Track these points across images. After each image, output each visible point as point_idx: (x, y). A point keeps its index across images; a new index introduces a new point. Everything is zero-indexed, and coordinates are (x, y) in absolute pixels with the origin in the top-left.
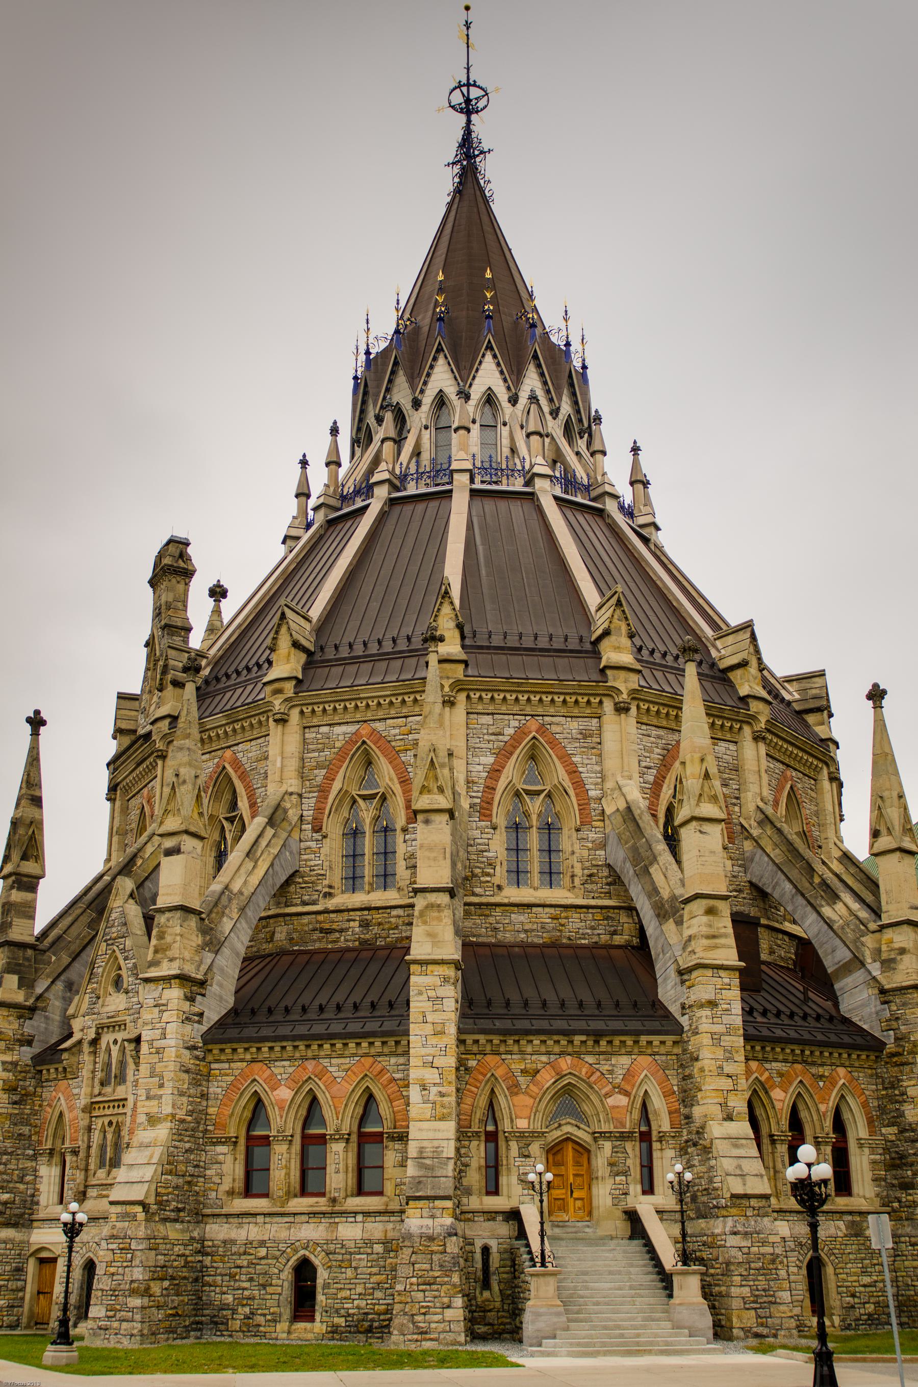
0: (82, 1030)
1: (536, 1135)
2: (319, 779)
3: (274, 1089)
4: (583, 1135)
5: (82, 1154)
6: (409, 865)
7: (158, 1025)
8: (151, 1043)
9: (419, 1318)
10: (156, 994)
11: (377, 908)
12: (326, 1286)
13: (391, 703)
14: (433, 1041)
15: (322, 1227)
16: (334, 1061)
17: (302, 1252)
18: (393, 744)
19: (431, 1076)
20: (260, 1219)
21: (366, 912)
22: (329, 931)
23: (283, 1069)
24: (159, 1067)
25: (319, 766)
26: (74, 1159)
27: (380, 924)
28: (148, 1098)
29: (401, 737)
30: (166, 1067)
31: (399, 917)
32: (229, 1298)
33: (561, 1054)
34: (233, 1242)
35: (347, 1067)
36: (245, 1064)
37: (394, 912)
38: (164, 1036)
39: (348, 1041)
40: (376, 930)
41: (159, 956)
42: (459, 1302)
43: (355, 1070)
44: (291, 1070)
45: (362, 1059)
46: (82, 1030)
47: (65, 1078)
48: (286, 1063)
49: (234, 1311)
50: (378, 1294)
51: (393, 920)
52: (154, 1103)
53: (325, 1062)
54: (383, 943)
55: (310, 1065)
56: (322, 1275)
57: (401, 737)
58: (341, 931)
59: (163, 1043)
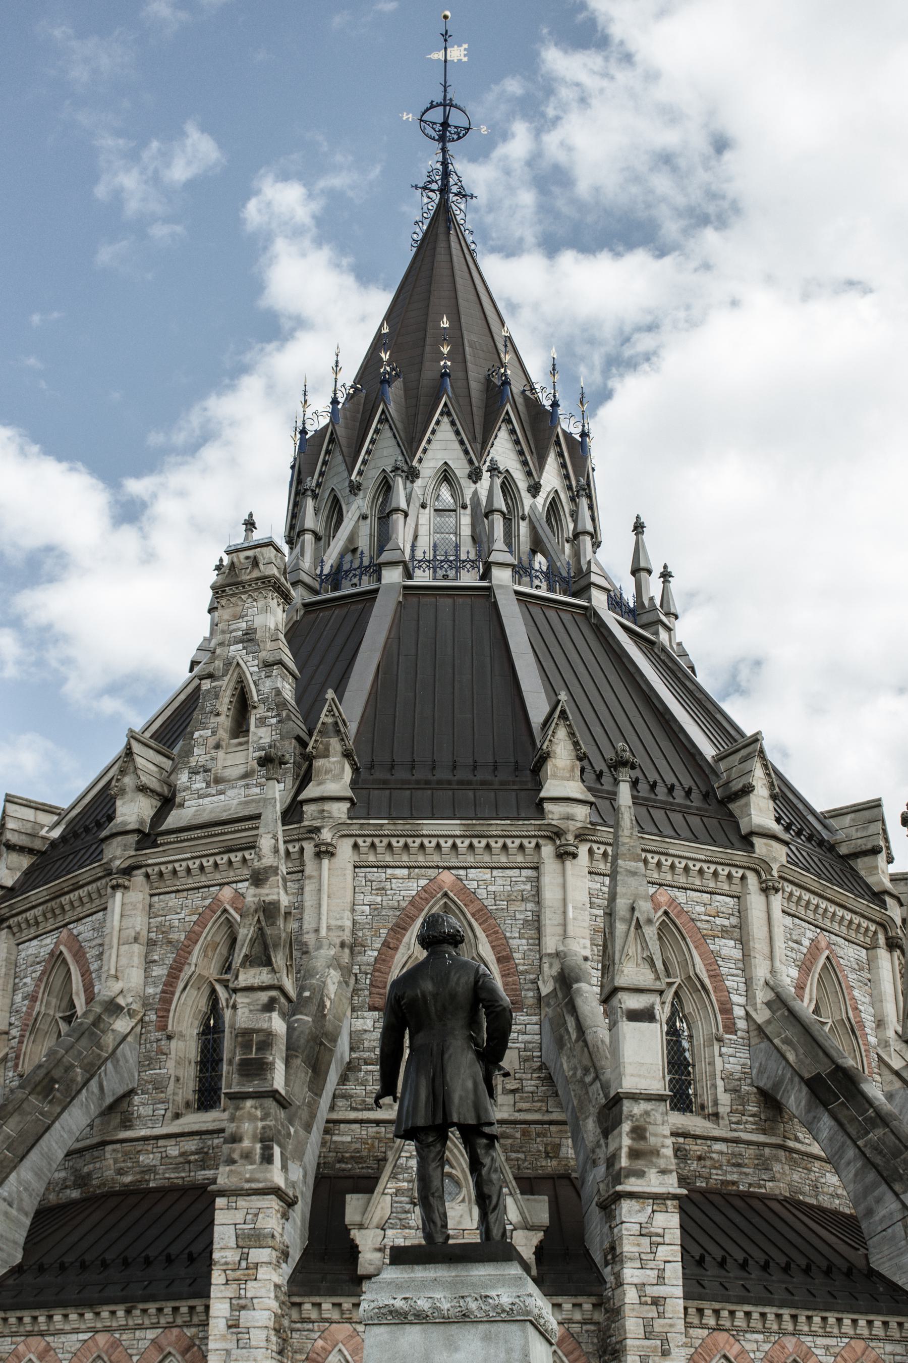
6: (728, 1087)
7: (652, 1264)
8: (640, 1287)
11: (696, 1137)
13: (701, 871)
16: (820, 1341)
18: (699, 924)
21: (681, 1140)
27: (700, 1158)
29: (708, 918)
30: (671, 1326)
31: (721, 1153)
35: (837, 1350)
36: (706, 1332)
37: (718, 1146)
38: (661, 1279)
39: (844, 1316)
40: (694, 1165)
41: (639, 1164)
43: (845, 1355)
44: (767, 1347)
45: (853, 1342)
47: (350, 1321)
48: (760, 1337)
51: (714, 1155)
54: (704, 1185)
55: (790, 1343)
57: (708, 918)
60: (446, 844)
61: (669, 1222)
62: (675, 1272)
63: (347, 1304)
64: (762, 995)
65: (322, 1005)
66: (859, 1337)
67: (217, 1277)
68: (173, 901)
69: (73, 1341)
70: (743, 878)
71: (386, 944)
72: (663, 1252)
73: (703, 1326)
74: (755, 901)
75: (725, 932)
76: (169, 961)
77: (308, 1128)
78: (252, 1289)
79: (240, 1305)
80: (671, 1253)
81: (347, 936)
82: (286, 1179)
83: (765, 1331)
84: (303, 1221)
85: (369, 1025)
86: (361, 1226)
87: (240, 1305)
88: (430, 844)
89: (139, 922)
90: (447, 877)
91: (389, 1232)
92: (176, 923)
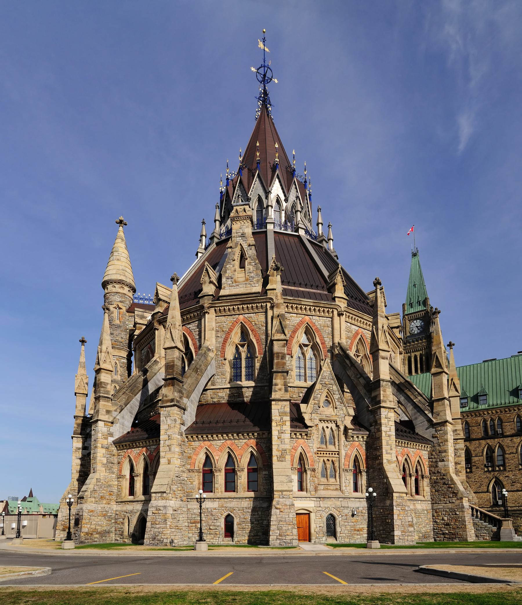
26: (313, 473)
47: (303, 438)
60: (308, 308)
67: (274, 424)
68: (223, 318)
69: (219, 443)
76: (224, 336)
78: (285, 428)
86: (305, 413)
88: (304, 307)
89: (214, 324)
91: (313, 415)
92: (225, 325)
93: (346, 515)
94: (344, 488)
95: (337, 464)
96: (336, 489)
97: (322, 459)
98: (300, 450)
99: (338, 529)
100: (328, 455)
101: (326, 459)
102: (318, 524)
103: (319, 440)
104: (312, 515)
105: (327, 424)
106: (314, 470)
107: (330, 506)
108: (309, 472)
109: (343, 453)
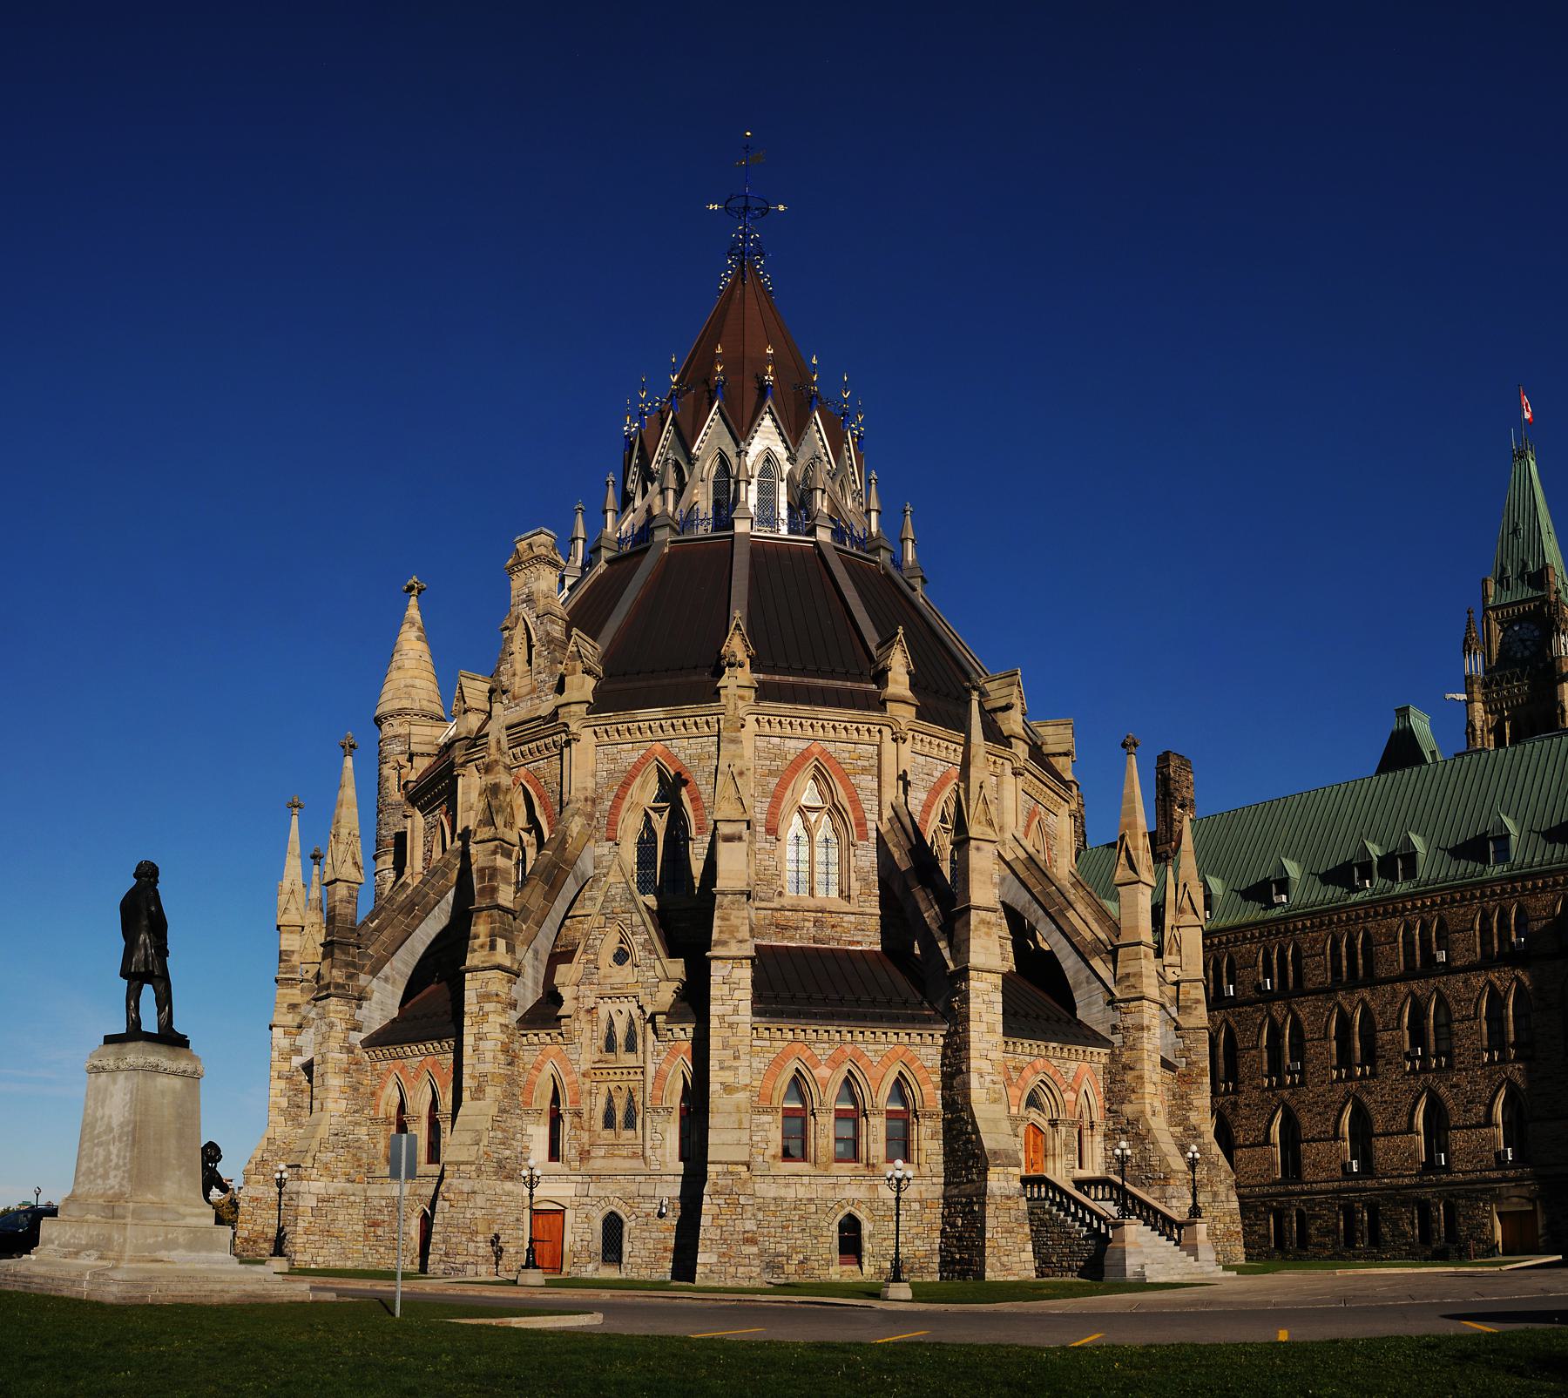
0: (577, 999)
1: (1023, 1119)
2: (772, 787)
3: (815, 1067)
4: (1043, 1123)
5: (586, 1116)
8: (722, 1017)
9: (1004, 1259)
10: (725, 972)
12: (871, 1236)
14: (988, 1037)
15: (863, 1188)
17: (848, 1209)
19: (986, 1066)
20: (806, 1180)
22: (785, 928)
23: (822, 1050)
24: (733, 1041)
25: (771, 773)
26: (576, 1120)
28: (721, 1068)
32: (784, 1249)
33: (1039, 1055)
34: (784, 1199)
38: (736, 1012)
40: (828, 931)
42: (1030, 1247)
46: (577, 999)
49: (789, 1258)
50: (917, 1242)
52: (727, 1073)
53: (862, 1047)
55: (848, 1049)
56: (867, 1228)
58: (796, 929)
59: (735, 1019)
61: (745, 974)
62: (746, 1007)
63: (554, 1033)
64: (888, 813)
65: (564, 841)
66: (900, 1043)
70: (880, 731)
71: (617, 796)
72: (737, 994)
73: (784, 1040)
74: (889, 747)
75: (864, 770)
77: (539, 924)
79: (480, 1037)
80: (745, 994)
81: (589, 794)
82: (514, 960)
83: (830, 1041)
84: (536, 984)
85: (606, 851)
86: (563, 985)
87: (480, 1037)
90: (658, 746)
93: (648, 1215)
94: (648, 1152)
95: (638, 1098)
96: (634, 1155)
97: (604, 1088)
98: (548, 1069)
99: (626, 1247)
100: (625, 1077)
101: (612, 1086)
102: (582, 1234)
103: (602, 1043)
104: (569, 1214)
105: (618, 1006)
106: (578, 1114)
107: (611, 1197)
108: (567, 1118)
109: (651, 1069)
